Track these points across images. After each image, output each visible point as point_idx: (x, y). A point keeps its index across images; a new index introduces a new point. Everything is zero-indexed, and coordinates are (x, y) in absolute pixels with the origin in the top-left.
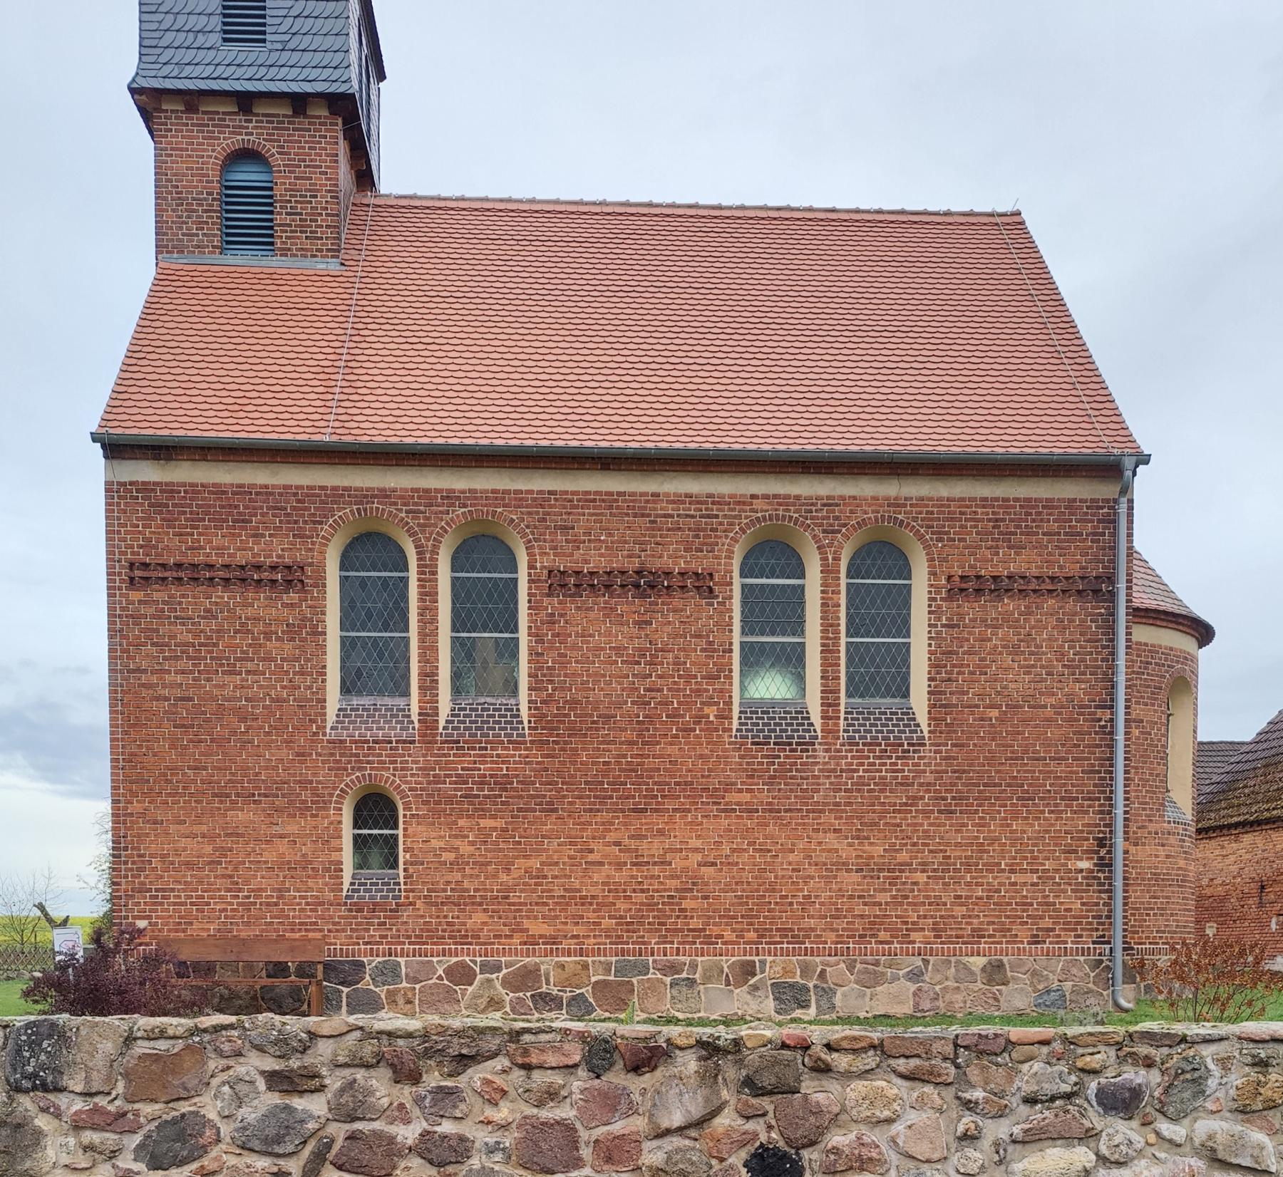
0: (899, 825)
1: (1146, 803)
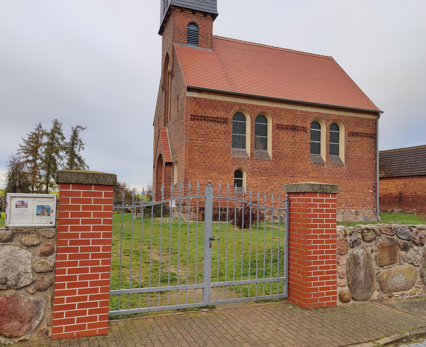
0: (339, 182)
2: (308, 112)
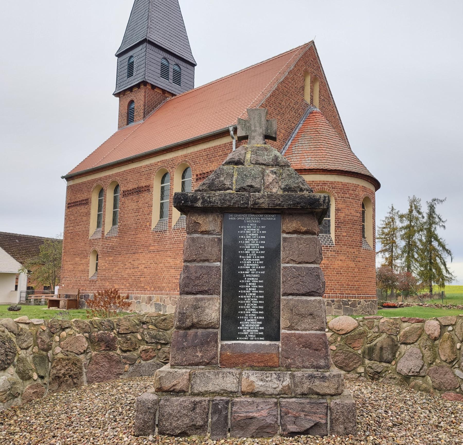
2: (151, 165)
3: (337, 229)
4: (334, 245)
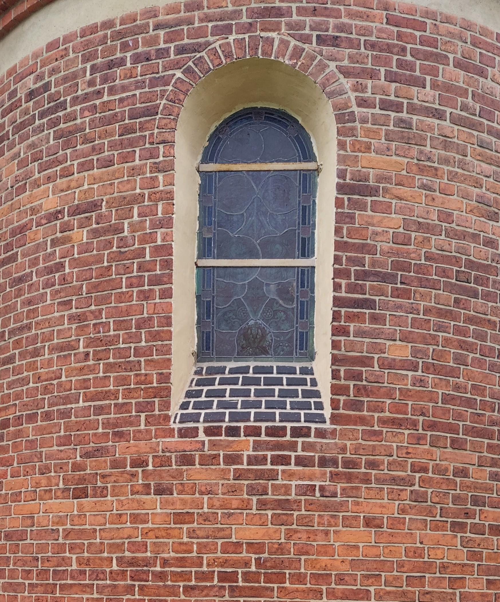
1: (106, 395)
3: (350, 318)
4: (328, 426)
